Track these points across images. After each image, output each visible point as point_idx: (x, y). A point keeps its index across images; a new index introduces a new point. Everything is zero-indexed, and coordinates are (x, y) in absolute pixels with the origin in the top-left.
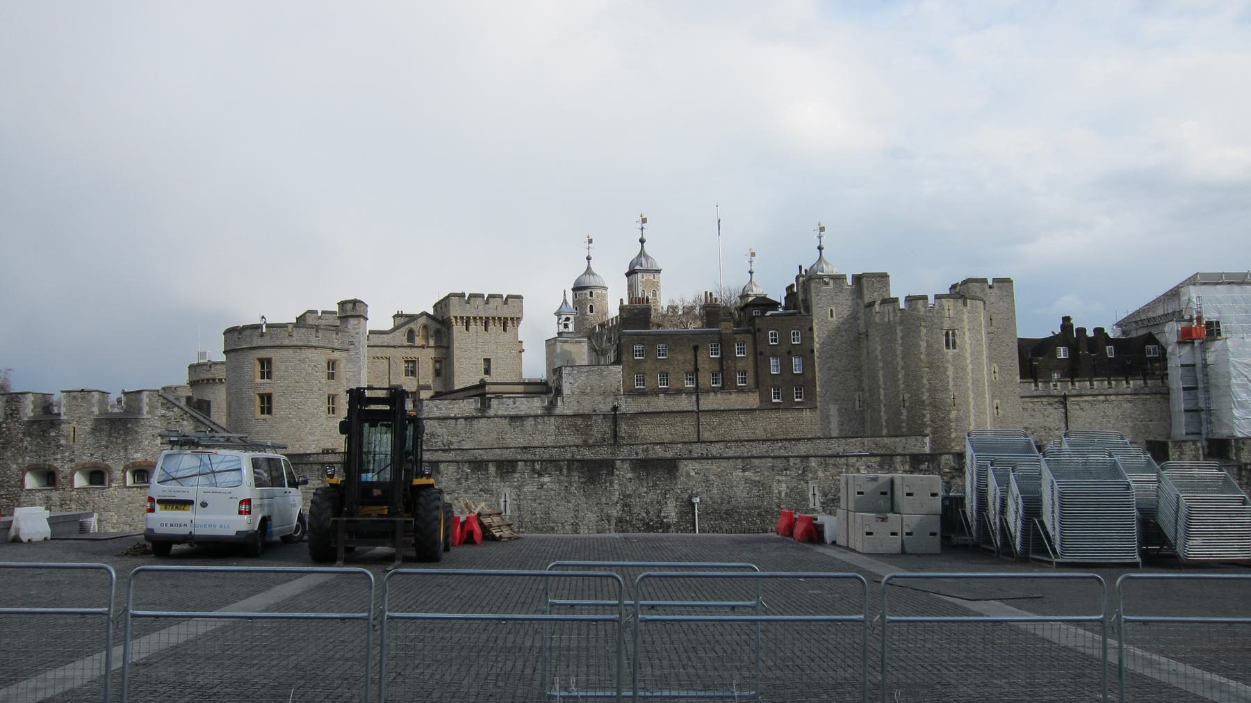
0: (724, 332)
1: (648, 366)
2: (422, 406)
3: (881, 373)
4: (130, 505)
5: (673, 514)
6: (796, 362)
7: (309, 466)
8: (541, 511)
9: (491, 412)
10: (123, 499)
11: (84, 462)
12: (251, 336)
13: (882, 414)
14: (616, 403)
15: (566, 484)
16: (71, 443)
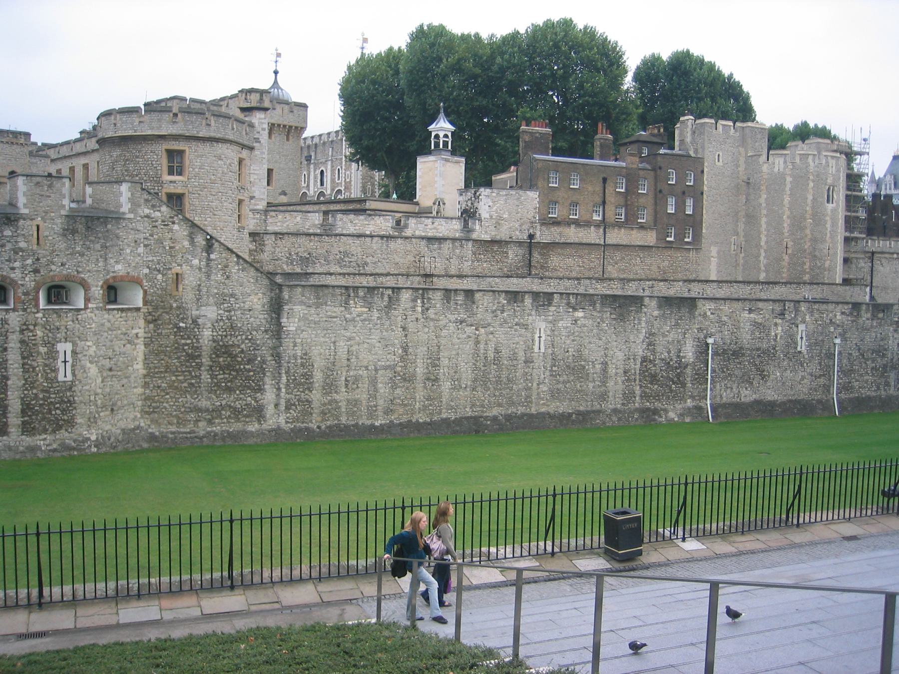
0: (631, 166)
1: (561, 195)
2: (335, 220)
3: (764, 220)
4: (110, 333)
5: (691, 354)
6: (689, 202)
7: (331, 290)
8: (573, 348)
9: (408, 232)
10: (103, 325)
11: (52, 273)
12: (159, 120)
13: (762, 258)
14: (531, 231)
15: (599, 320)
16: (35, 247)
